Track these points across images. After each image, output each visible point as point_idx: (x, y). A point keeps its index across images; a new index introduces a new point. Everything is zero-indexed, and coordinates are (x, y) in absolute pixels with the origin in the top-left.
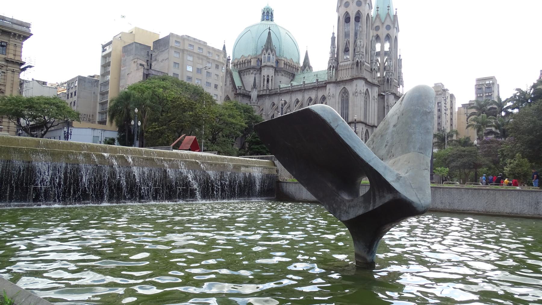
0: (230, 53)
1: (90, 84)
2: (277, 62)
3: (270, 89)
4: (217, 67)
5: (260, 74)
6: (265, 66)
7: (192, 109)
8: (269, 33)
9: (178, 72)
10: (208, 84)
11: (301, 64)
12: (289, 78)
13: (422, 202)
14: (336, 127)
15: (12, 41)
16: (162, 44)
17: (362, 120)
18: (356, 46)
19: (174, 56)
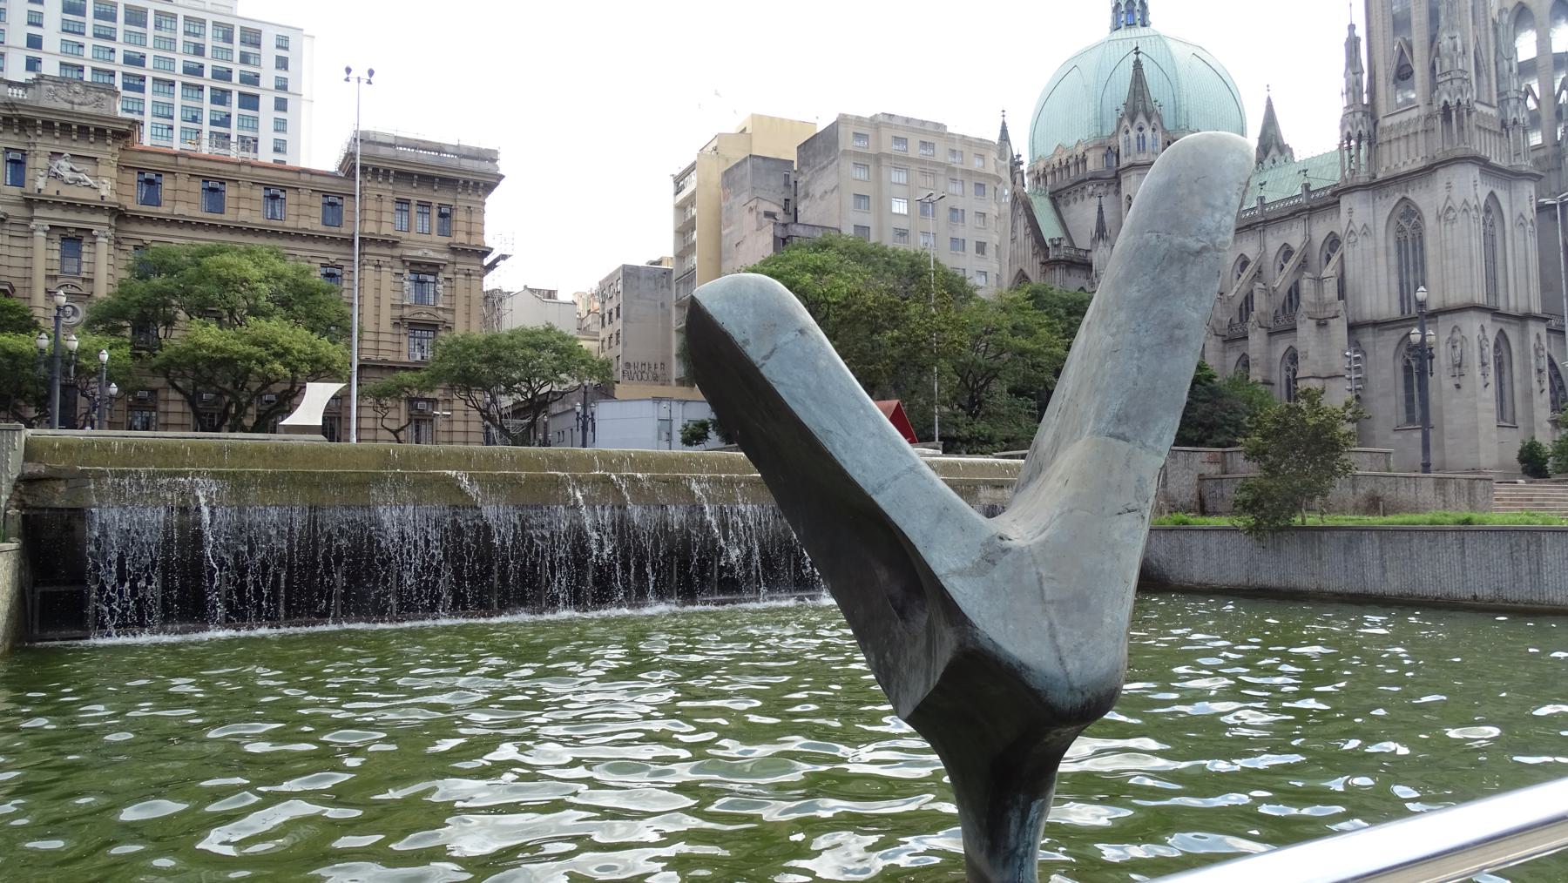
0: (1020, 145)
1: (651, 284)
5: (1118, 192)
6: (1132, 166)
8: (1138, 65)
9: (867, 219)
10: (957, 244)
11: (1252, 140)
13: (1073, 665)
14: (767, 358)
15: (462, 200)
16: (819, 147)
17: (1480, 298)
18: (1438, 54)
19: (854, 177)
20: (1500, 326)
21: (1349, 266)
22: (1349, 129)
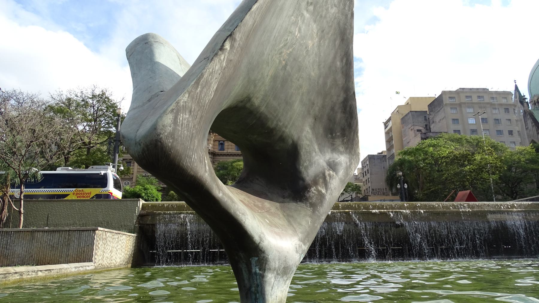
0: (525, 92)
1: (379, 161)
4: (507, 110)
7: (470, 162)
10: (500, 132)
16: (436, 104)
19: (451, 113)
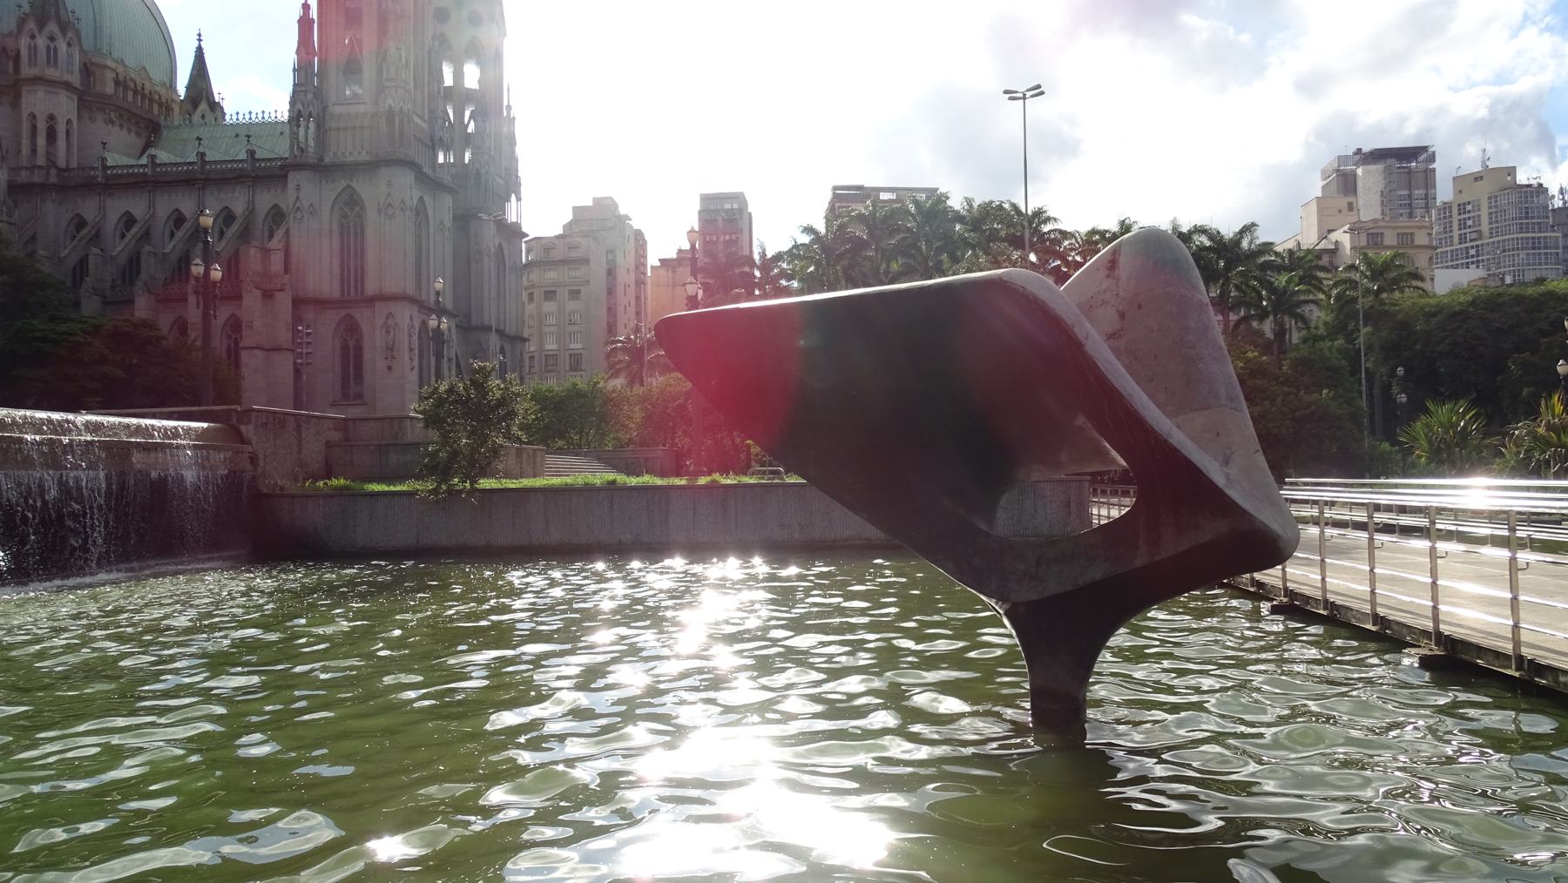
2: (87, 70)
3: (62, 163)
5: (15, 105)
11: (181, 90)
12: (138, 135)
17: (410, 289)
20: (423, 317)
21: (295, 242)
22: (299, 106)
